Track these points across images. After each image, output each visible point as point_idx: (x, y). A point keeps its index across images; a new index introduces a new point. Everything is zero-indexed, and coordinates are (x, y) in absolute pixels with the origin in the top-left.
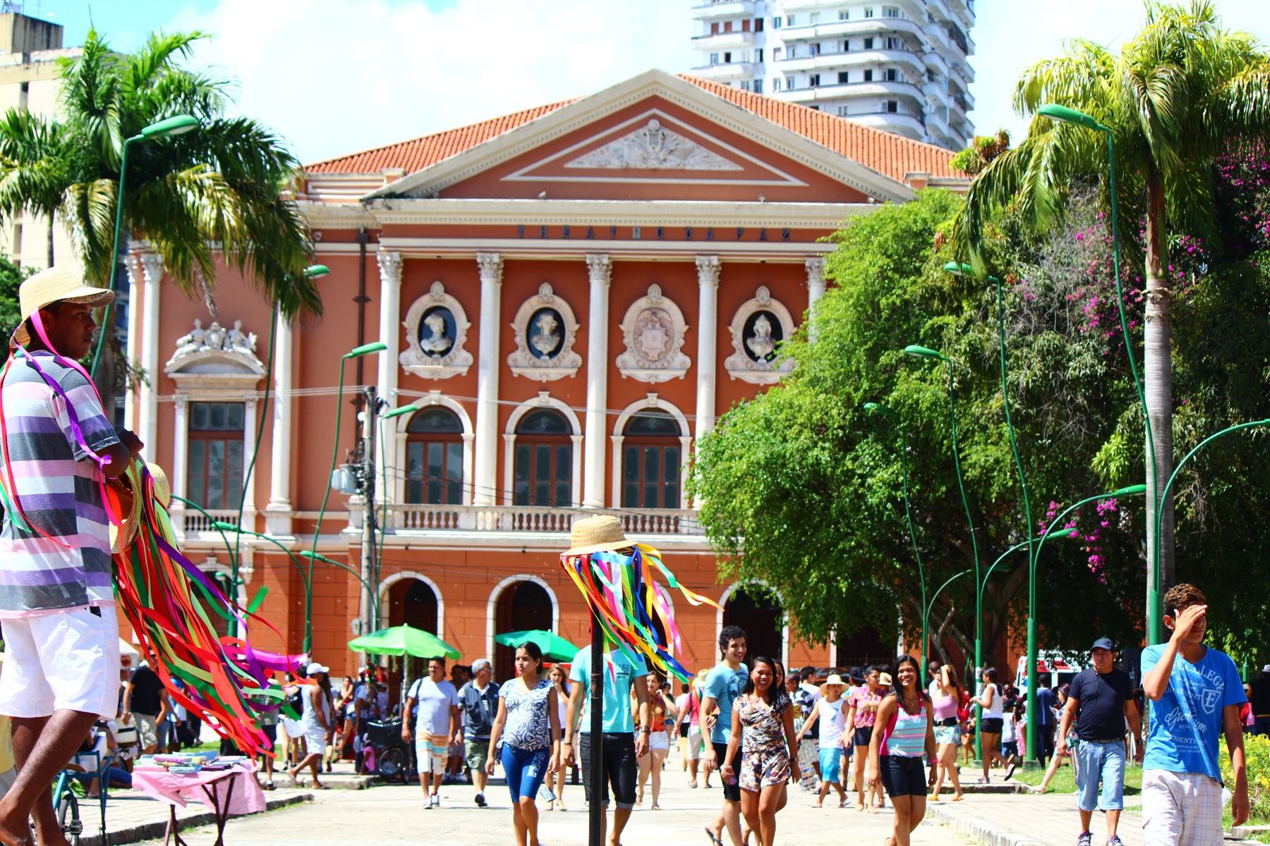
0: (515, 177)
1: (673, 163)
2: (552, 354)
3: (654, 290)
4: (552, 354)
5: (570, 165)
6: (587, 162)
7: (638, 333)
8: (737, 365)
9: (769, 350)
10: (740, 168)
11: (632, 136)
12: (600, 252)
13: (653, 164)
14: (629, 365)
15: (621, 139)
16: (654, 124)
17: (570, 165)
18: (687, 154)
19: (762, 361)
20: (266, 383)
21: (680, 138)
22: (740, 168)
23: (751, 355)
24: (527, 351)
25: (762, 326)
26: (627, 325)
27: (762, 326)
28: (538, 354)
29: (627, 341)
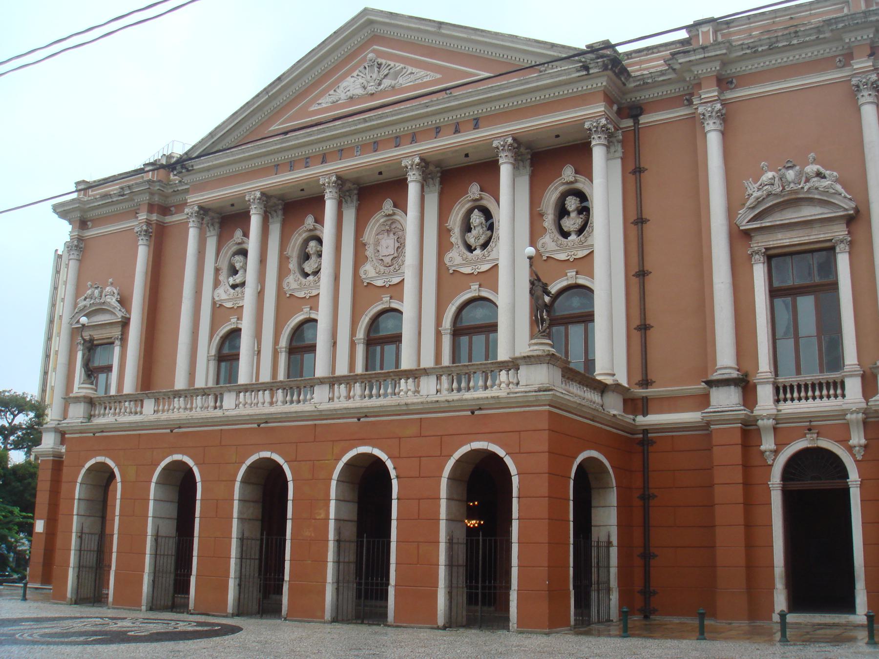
0: (275, 127)
1: (387, 83)
5: (312, 109)
6: (325, 101)
7: (377, 243)
8: (456, 257)
9: (482, 241)
10: (439, 76)
11: (355, 74)
12: (329, 175)
13: (371, 89)
14: (369, 271)
15: (349, 79)
16: (371, 55)
17: (312, 109)
18: (396, 75)
20: (125, 323)
21: (392, 64)
22: (439, 76)
23: (470, 249)
26: (369, 235)
29: (370, 252)
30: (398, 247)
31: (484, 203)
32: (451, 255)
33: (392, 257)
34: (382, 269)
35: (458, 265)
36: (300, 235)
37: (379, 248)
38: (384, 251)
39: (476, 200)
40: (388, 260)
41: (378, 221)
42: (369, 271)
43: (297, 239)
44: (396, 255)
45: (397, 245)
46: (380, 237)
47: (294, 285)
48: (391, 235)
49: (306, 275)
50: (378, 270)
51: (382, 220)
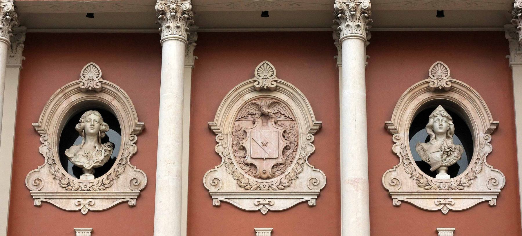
2: (98, 172)
3: (266, 73)
4: (98, 172)
8: (402, 180)
14: (223, 181)
19: (443, 176)
24: (59, 165)
25: (440, 119)
26: (225, 119)
27: (440, 119)
28: (78, 171)
29: (225, 146)
30: (286, 148)
31: (455, 96)
32: (394, 175)
33: (274, 162)
34: (254, 181)
35: (411, 193)
36: (66, 96)
37: (247, 144)
38: (254, 150)
39: (443, 90)
40: (266, 166)
41: (241, 96)
42: (223, 181)
43: (59, 103)
44: (280, 161)
45: (283, 143)
46: (245, 125)
47: (49, 185)
48: (271, 124)
49: (78, 171)
50: (244, 182)
51: (248, 97)
